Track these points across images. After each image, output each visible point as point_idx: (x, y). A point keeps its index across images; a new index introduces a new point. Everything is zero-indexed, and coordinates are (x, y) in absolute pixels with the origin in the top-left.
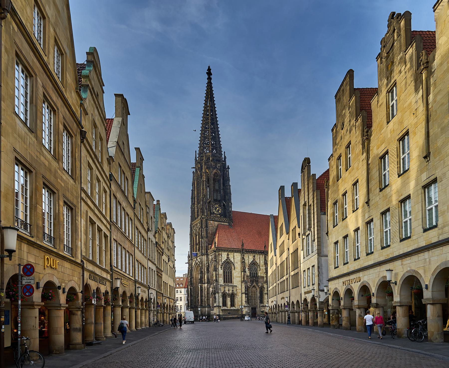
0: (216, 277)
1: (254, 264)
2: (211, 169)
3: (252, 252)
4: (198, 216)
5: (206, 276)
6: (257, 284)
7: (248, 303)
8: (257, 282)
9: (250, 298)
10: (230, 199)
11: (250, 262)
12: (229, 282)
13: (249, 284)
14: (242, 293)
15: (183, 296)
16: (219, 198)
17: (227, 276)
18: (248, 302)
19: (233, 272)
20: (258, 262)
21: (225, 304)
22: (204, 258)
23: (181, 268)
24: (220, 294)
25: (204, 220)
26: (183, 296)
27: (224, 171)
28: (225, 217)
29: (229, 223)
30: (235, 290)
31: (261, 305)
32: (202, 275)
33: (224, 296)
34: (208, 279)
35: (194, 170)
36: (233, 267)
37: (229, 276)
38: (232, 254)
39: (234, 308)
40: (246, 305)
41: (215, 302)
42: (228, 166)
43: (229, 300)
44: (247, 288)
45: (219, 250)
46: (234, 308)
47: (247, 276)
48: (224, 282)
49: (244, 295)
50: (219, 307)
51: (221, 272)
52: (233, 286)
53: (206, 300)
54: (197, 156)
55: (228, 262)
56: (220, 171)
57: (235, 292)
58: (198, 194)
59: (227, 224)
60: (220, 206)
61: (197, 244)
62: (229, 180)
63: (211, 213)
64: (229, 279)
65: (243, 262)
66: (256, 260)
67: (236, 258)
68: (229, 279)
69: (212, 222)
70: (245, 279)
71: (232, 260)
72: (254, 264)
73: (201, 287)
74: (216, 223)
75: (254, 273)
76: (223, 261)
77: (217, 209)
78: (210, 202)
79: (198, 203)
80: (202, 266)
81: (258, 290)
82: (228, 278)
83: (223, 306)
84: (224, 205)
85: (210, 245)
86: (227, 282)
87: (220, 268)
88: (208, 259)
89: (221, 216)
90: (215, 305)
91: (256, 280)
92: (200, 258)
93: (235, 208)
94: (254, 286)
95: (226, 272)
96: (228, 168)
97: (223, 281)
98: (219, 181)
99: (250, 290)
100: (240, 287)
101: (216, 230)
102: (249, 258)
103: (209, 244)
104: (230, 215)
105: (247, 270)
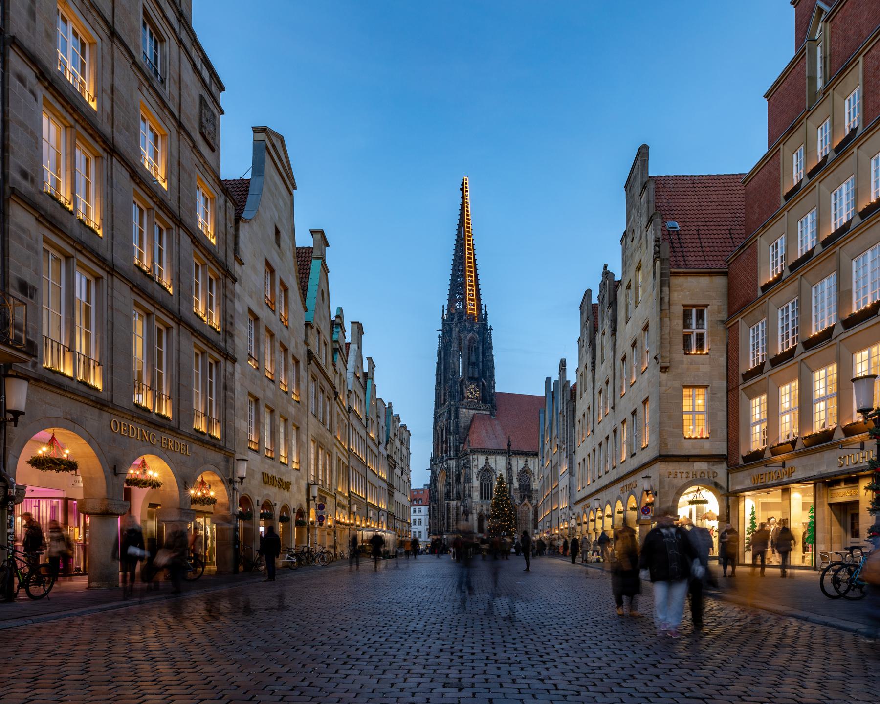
0: (469, 491)
2: (466, 333)
4: (445, 401)
5: (455, 490)
6: (530, 501)
8: (530, 498)
10: (492, 376)
11: (520, 469)
15: (423, 518)
16: (476, 375)
20: (532, 469)
22: (453, 463)
23: (419, 475)
25: (453, 409)
26: (423, 518)
27: (484, 334)
31: (536, 531)
34: (458, 493)
35: (441, 333)
45: (475, 451)
48: (481, 498)
51: (476, 483)
54: (446, 312)
56: (478, 334)
58: (445, 368)
60: (478, 386)
61: (443, 443)
62: (490, 347)
65: (509, 469)
67: (499, 464)
71: (493, 466)
73: (448, 505)
74: (472, 412)
76: (480, 467)
77: (472, 392)
78: (462, 381)
79: (446, 382)
81: (532, 509)
83: (479, 532)
84: (483, 384)
93: (499, 388)
96: (491, 329)
97: (479, 497)
98: (477, 349)
101: (472, 421)
103: (460, 443)
104: (492, 400)
105: (515, 480)
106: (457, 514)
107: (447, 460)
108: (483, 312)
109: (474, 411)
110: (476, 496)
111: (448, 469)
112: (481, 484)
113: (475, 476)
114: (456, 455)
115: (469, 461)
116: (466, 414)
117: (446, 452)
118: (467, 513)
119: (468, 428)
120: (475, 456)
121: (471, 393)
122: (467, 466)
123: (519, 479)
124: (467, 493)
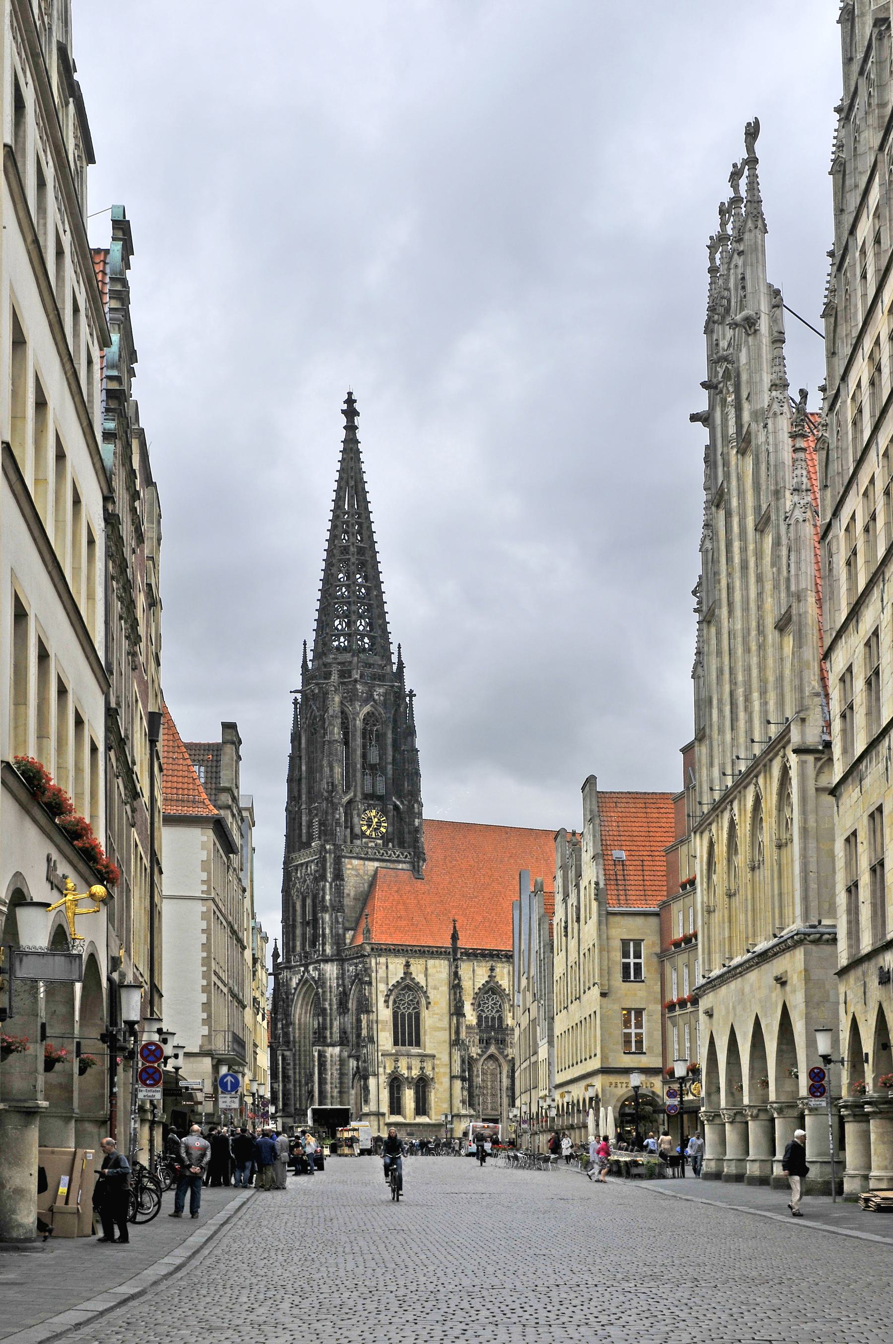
1: (491, 989)
3: (483, 956)
7: (471, 1105)
9: (477, 1092)
12: (410, 1044)
13: (475, 1051)
14: (452, 1078)
16: (381, 790)
17: (403, 1025)
18: (470, 1102)
19: (425, 1014)
21: (396, 1107)
22: (331, 970)
24: (383, 1079)
28: (402, 844)
29: (412, 863)
30: (428, 1066)
32: (324, 1020)
33: (395, 1083)
36: (423, 1001)
37: (410, 1026)
38: (422, 961)
39: (423, 1119)
40: (463, 1112)
41: (367, 1102)
42: (411, 691)
43: (409, 1097)
44: (468, 1063)
46: (423, 1119)
47: (469, 1027)
48: (396, 1043)
49: (458, 1084)
50: (379, 1115)
51: (385, 1014)
52: (423, 1057)
53: (335, 1094)
55: (408, 987)
57: (429, 1072)
59: (405, 866)
60: (384, 812)
62: (411, 732)
63: (354, 836)
64: (410, 1034)
65: (456, 986)
66: (498, 979)
67: (434, 975)
68: (410, 1034)
69: (356, 862)
70: (463, 1035)
71: (420, 979)
72: (491, 989)
73: (321, 1055)
74: (372, 865)
75: (493, 1018)
76: (393, 982)
80: (324, 992)
82: (408, 1031)
83: (392, 1112)
84: (396, 807)
85: (351, 933)
86: (403, 1044)
87: (381, 1004)
88: (343, 974)
89: (385, 844)
90: (366, 1110)
91: (497, 1040)
92: (315, 969)
94: (491, 1057)
95: (403, 1015)
96: (411, 695)
97: (391, 1040)
98: (380, 737)
99: (478, 1067)
100: (445, 1058)
102: (475, 976)
103: (347, 929)
104: (416, 840)
105: (468, 1009)
106: (342, 1075)
107: (318, 962)
108: (394, 659)
109: (376, 864)
110: (385, 1039)
111: (321, 981)
112: (395, 1015)
113: (381, 999)
114: (339, 952)
115: (367, 971)
116: (357, 871)
117: (315, 946)
118: (363, 1075)
119: (365, 898)
120: (382, 960)
121: (369, 826)
122: (363, 979)
123: (478, 1005)
124: (364, 1032)
